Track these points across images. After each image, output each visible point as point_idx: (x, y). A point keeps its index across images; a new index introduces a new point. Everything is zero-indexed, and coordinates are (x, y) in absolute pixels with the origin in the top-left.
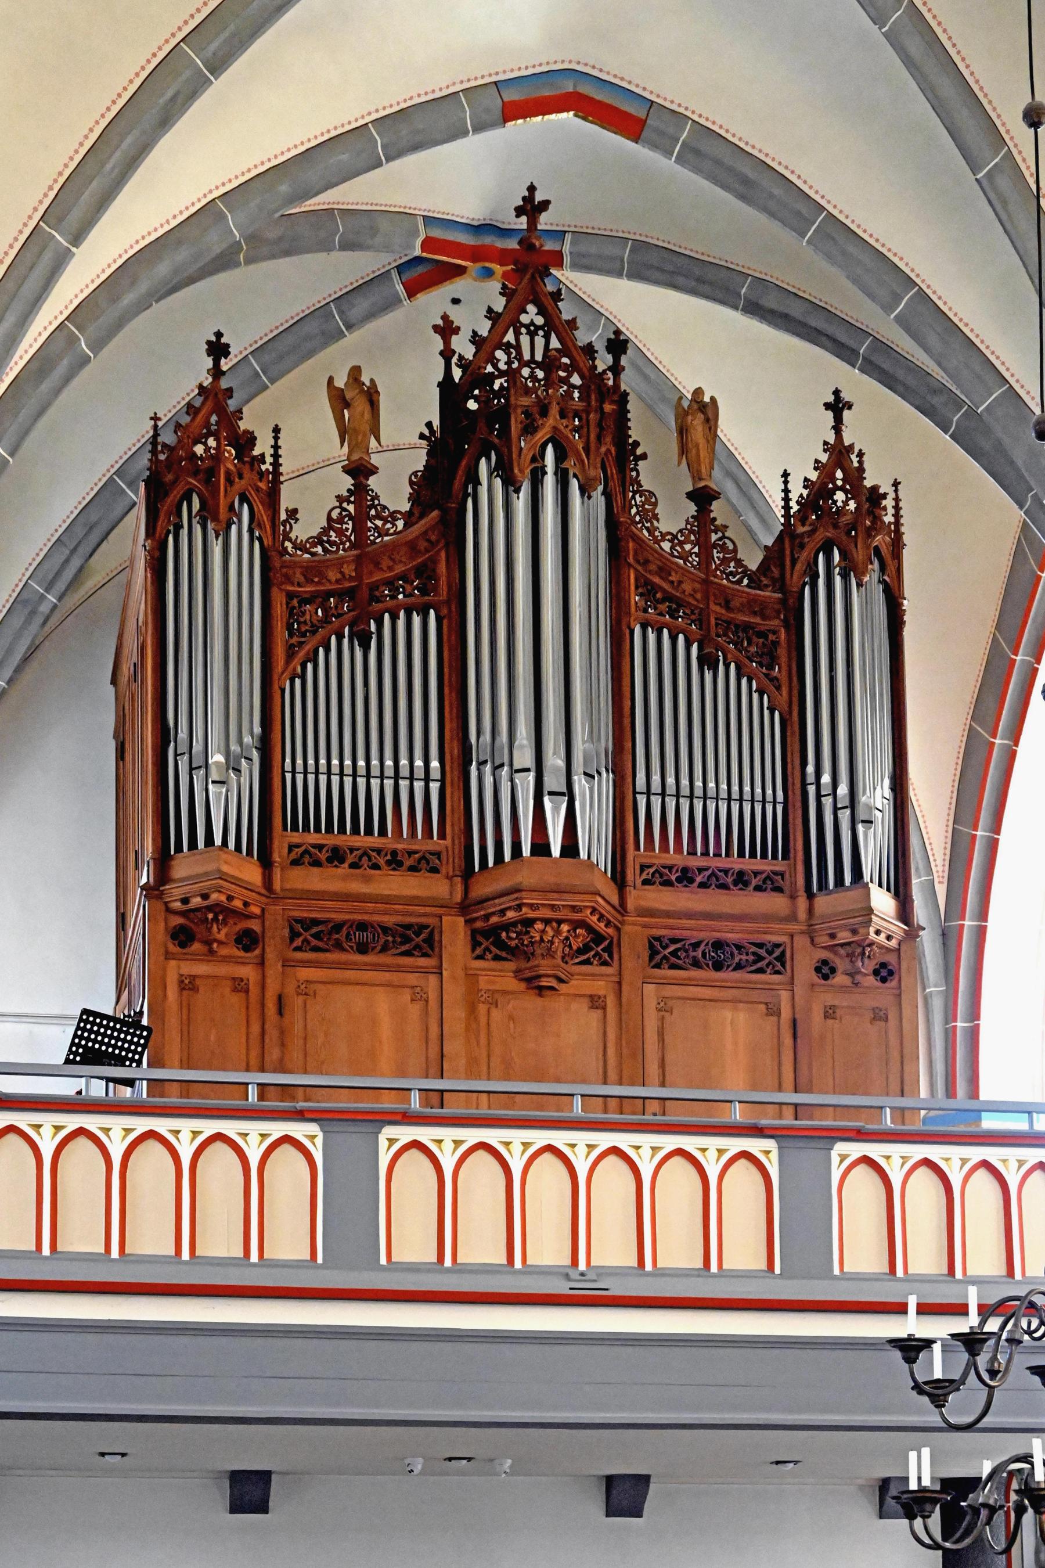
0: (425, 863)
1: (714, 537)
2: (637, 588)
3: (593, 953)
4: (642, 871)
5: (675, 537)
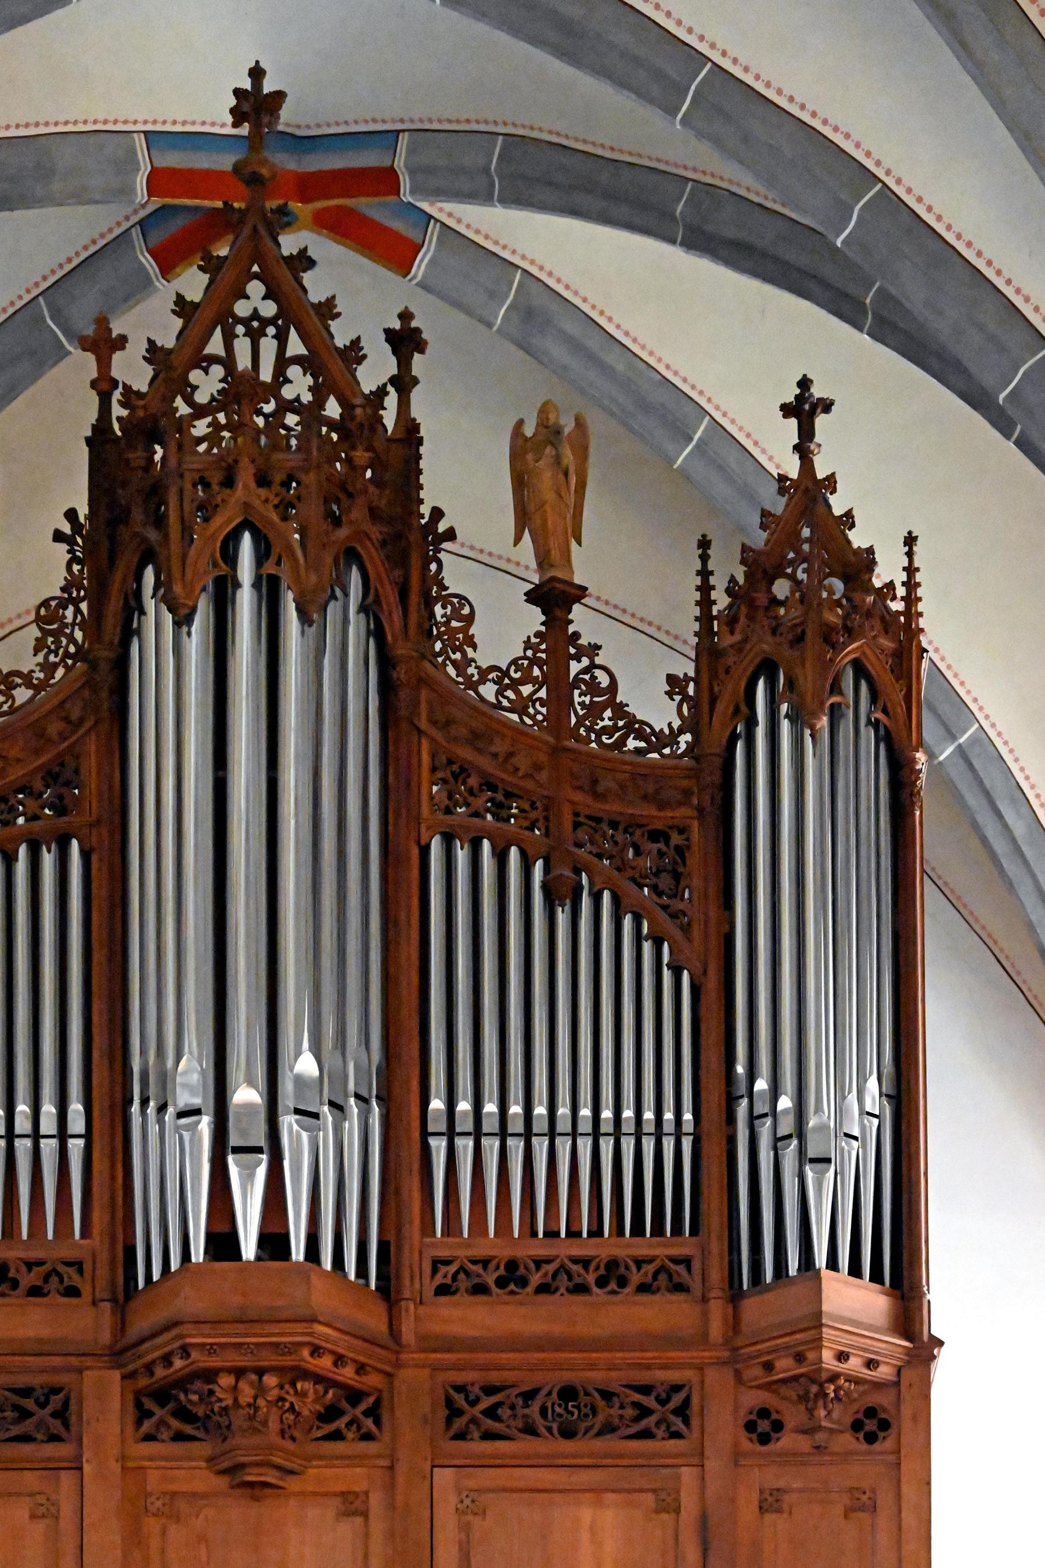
0: (55, 1281)
1: (575, 667)
2: (434, 769)
3: (345, 1419)
4: (435, 1271)
5: (506, 674)
